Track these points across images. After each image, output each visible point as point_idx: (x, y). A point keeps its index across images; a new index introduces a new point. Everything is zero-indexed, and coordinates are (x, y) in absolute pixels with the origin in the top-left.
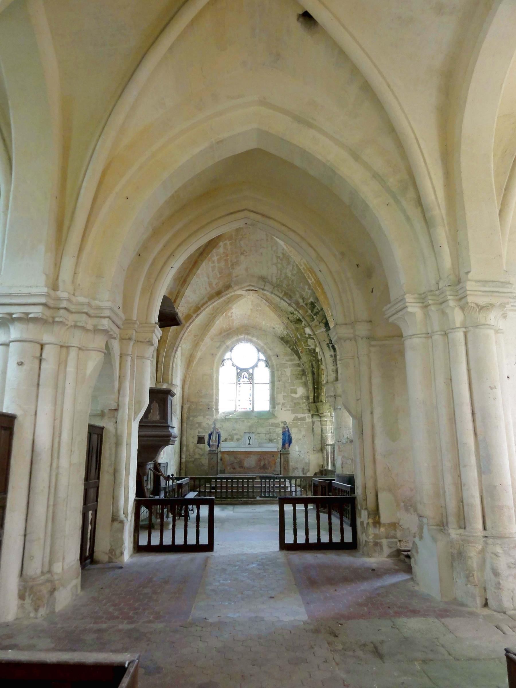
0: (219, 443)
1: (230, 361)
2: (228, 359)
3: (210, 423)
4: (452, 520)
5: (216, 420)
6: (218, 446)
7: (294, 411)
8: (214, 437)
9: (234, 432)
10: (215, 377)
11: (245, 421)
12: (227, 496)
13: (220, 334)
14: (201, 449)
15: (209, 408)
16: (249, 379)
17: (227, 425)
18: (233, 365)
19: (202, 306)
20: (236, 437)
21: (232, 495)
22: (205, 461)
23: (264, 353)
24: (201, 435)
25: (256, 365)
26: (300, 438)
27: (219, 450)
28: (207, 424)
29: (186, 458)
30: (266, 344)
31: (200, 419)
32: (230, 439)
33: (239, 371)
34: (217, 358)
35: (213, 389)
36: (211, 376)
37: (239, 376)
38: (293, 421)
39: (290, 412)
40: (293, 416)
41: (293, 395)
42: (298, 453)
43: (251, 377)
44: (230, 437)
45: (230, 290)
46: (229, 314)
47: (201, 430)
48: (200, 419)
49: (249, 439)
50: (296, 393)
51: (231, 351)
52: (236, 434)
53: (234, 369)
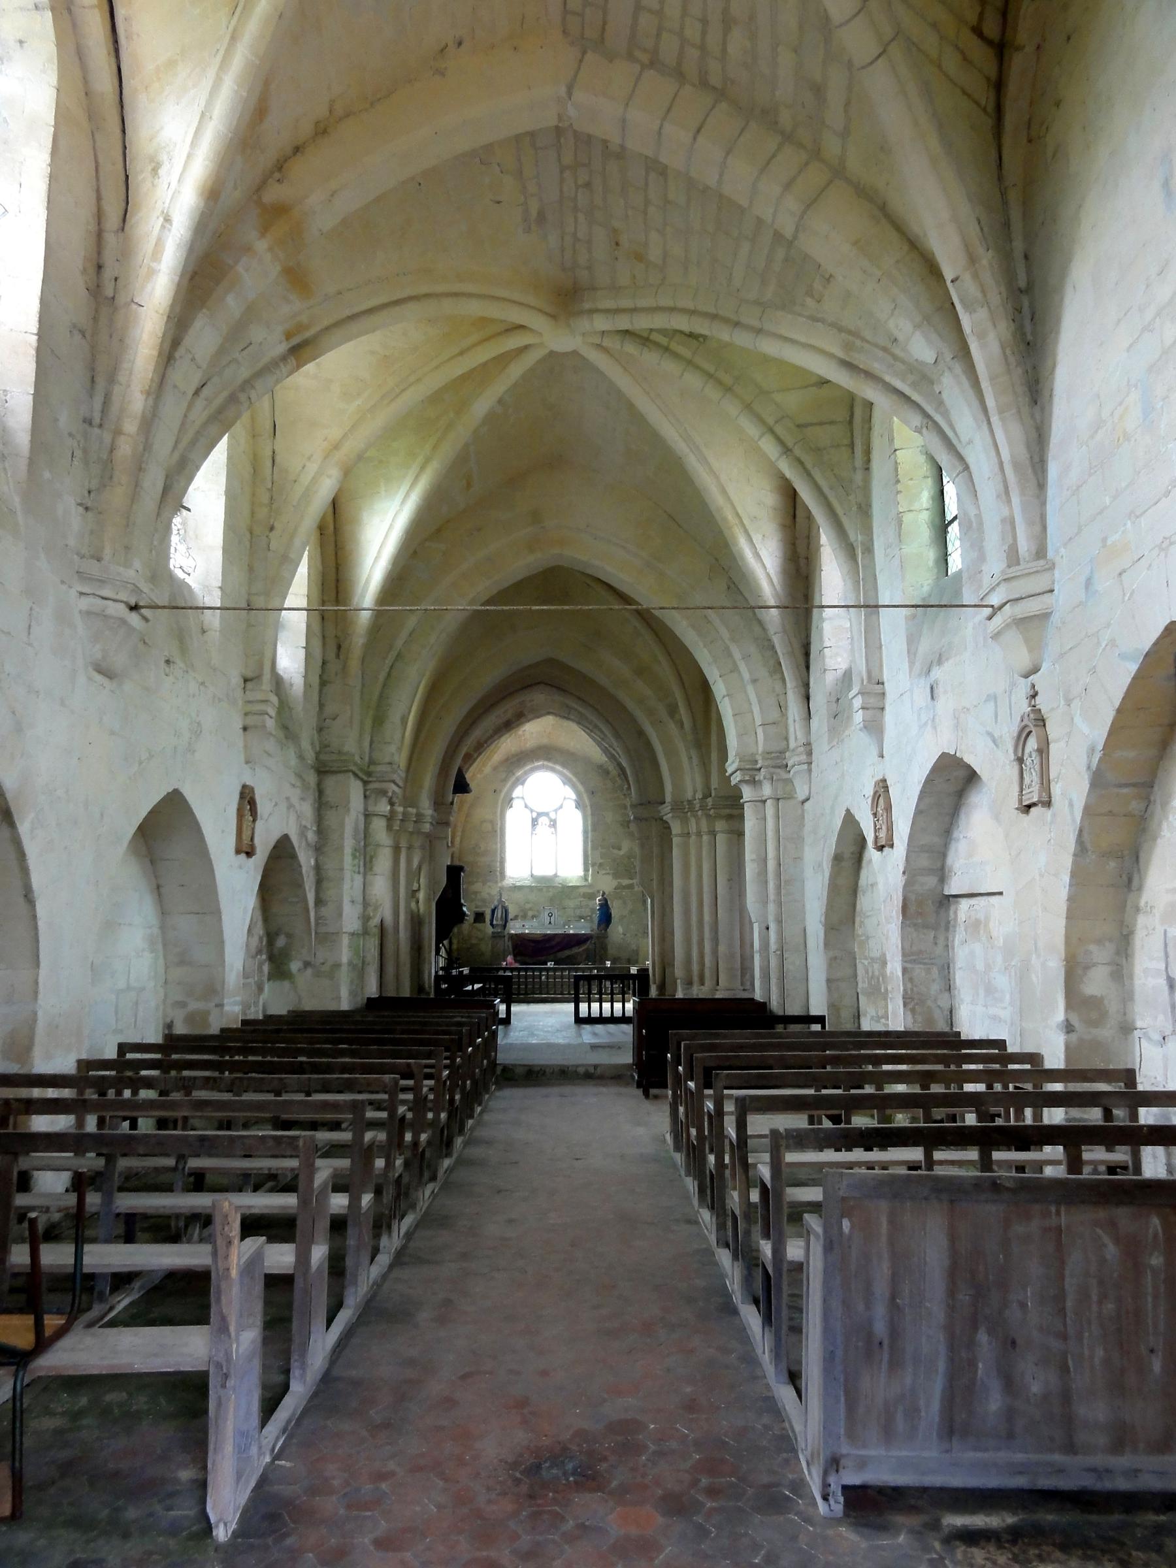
0: (506, 921)
1: (521, 800)
2: (518, 798)
3: (494, 892)
4: (696, 979)
5: (502, 888)
6: (505, 926)
7: (616, 875)
8: (499, 913)
9: (527, 906)
10: (499, 824)
11: (545, 890)
12: (519, 992)
13: (507, 760)
14: (480, 930)
15: (491, 872)
16: (550, 826)
17: (518, 896)
18: (526, 806)
19: (486, 742)
20: (530, 913)
21: (526, 991)
22: (486, 948)
23: (574, 787)
24: (480, 910)
25: (561, 807)
26: (624, 914)
27: (506, 932)
28: (489, 894)
29: (458, 942)
30: (575, 774)
31: (477, 886)
32: (522, 916)
33: (535, 815)
34: (503, 794)
35: (496, 844)
36: (492, 822)
37: (534, 822)
38: (615, 889)
39: (610, 877)
40: (615, 883)
41: (616, 851)
42: (622, 936)
43: (553, 824)
44: (521, 914)
45: (523, 720)
46: (520, 732)
47: (479, 904)
48: (477, 886)
49: (550, 917)
50: (620, 849)
51: (523, 784)
52: (530, 909)
53: (528, 811)
